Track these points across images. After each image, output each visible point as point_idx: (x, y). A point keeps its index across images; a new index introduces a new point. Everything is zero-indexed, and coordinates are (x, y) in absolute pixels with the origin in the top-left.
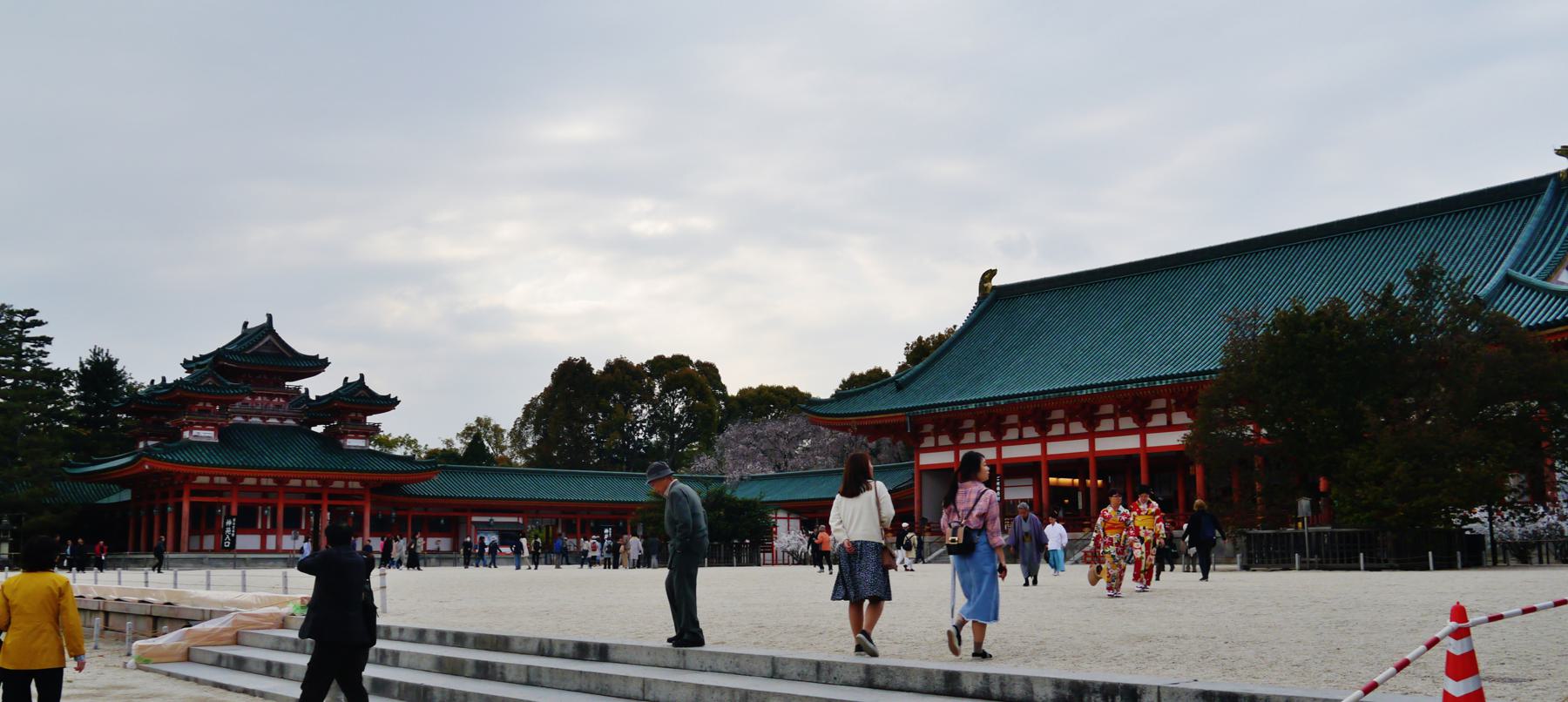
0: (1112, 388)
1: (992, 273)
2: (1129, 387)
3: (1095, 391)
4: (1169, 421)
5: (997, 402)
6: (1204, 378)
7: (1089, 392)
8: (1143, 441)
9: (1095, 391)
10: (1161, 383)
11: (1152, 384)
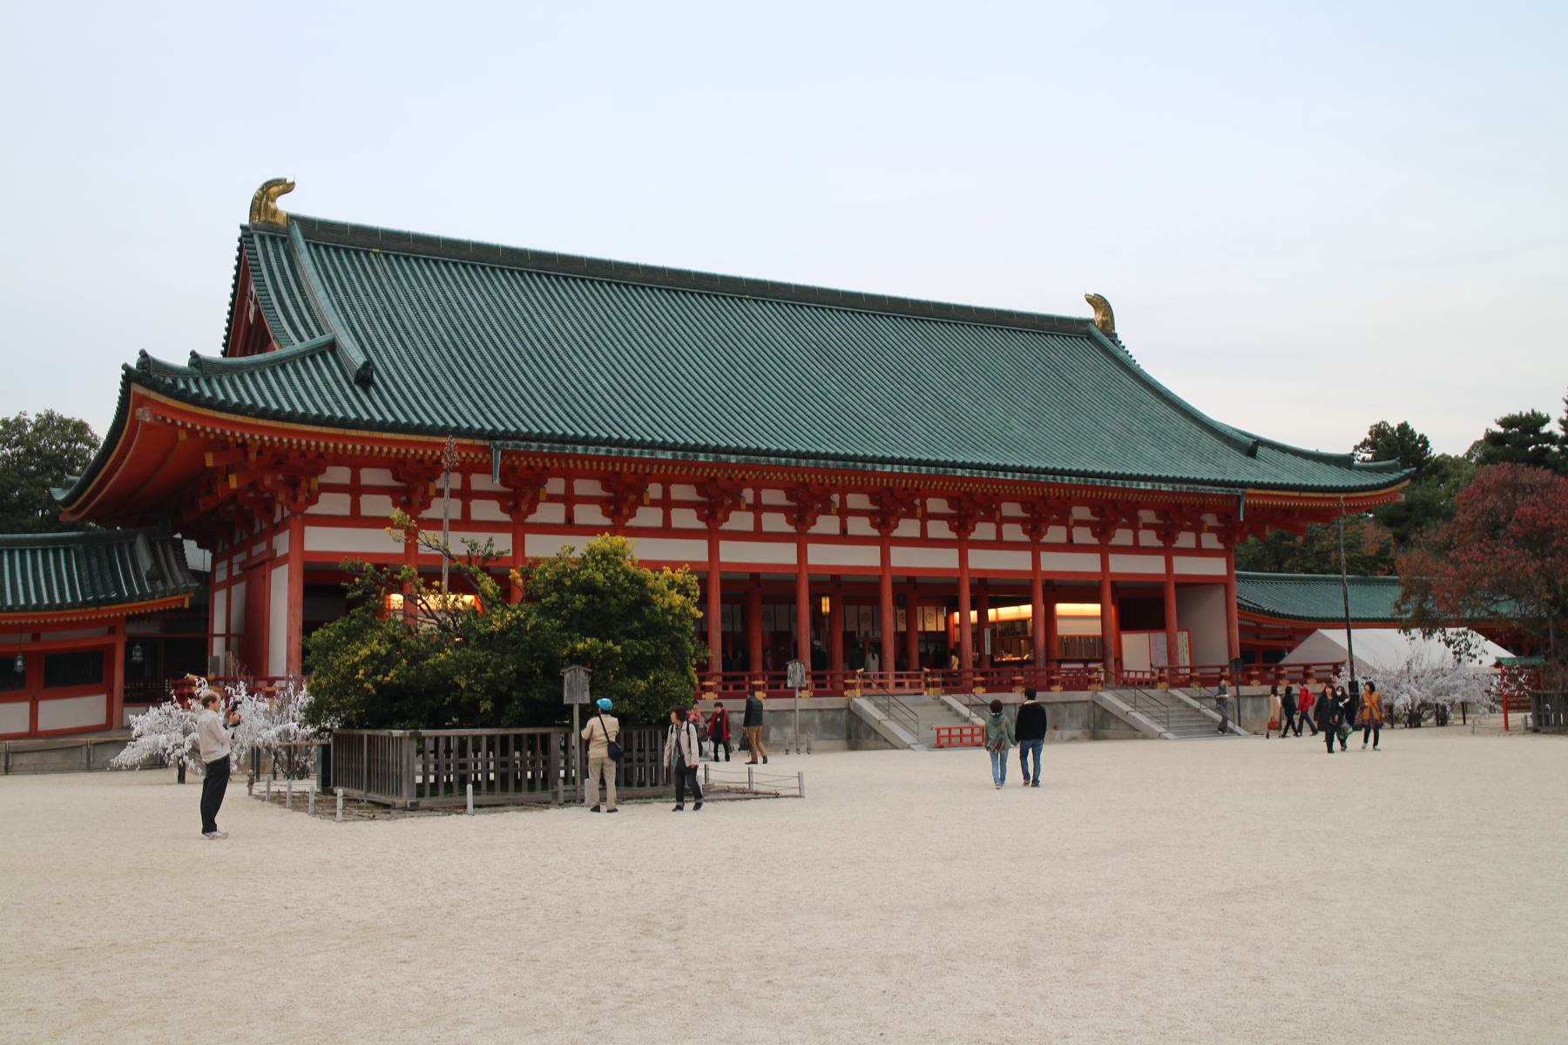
0: (933, 470)
1: (286, 187)
2: (959, 472)
3: (906, 469)
4: (1070, 538)
5: (723, 457)
6: (1063, 480)
7: (896, 469)
8: (885, 556)
9: (906, 469)
10: (1006, 476)
11: (992, 475)
